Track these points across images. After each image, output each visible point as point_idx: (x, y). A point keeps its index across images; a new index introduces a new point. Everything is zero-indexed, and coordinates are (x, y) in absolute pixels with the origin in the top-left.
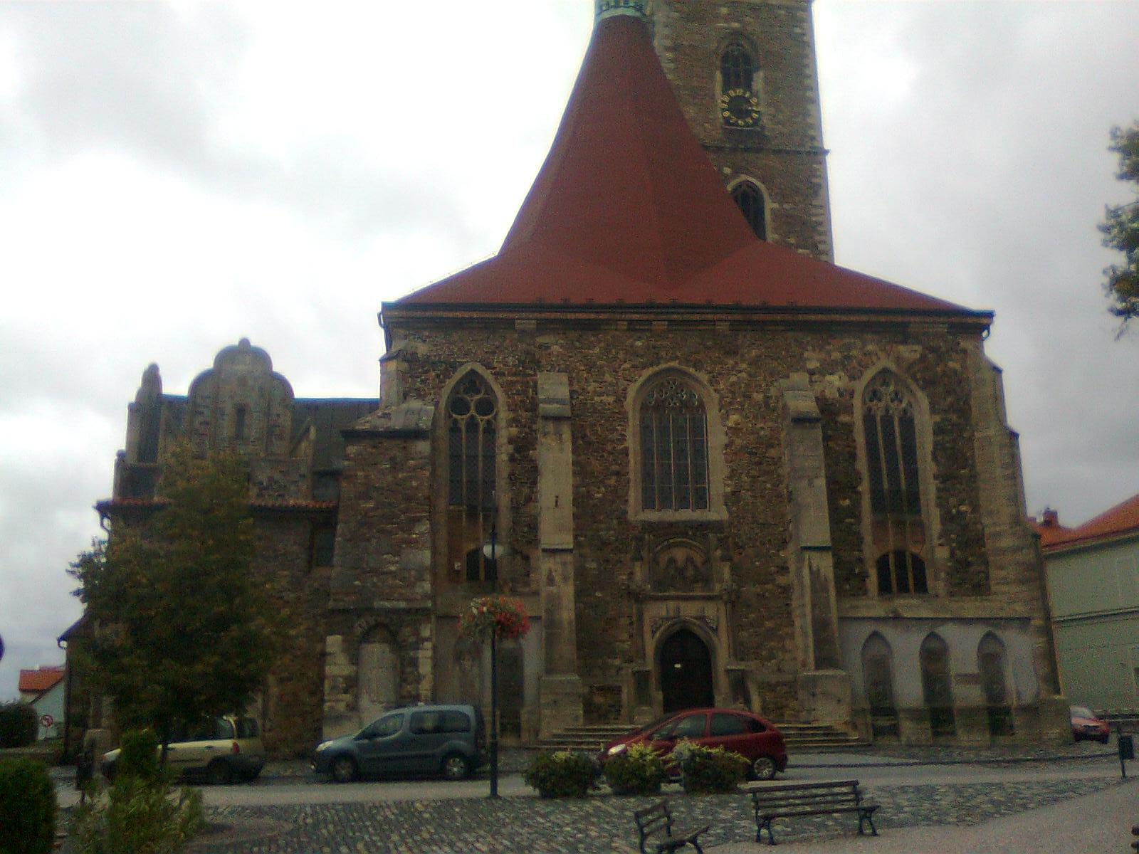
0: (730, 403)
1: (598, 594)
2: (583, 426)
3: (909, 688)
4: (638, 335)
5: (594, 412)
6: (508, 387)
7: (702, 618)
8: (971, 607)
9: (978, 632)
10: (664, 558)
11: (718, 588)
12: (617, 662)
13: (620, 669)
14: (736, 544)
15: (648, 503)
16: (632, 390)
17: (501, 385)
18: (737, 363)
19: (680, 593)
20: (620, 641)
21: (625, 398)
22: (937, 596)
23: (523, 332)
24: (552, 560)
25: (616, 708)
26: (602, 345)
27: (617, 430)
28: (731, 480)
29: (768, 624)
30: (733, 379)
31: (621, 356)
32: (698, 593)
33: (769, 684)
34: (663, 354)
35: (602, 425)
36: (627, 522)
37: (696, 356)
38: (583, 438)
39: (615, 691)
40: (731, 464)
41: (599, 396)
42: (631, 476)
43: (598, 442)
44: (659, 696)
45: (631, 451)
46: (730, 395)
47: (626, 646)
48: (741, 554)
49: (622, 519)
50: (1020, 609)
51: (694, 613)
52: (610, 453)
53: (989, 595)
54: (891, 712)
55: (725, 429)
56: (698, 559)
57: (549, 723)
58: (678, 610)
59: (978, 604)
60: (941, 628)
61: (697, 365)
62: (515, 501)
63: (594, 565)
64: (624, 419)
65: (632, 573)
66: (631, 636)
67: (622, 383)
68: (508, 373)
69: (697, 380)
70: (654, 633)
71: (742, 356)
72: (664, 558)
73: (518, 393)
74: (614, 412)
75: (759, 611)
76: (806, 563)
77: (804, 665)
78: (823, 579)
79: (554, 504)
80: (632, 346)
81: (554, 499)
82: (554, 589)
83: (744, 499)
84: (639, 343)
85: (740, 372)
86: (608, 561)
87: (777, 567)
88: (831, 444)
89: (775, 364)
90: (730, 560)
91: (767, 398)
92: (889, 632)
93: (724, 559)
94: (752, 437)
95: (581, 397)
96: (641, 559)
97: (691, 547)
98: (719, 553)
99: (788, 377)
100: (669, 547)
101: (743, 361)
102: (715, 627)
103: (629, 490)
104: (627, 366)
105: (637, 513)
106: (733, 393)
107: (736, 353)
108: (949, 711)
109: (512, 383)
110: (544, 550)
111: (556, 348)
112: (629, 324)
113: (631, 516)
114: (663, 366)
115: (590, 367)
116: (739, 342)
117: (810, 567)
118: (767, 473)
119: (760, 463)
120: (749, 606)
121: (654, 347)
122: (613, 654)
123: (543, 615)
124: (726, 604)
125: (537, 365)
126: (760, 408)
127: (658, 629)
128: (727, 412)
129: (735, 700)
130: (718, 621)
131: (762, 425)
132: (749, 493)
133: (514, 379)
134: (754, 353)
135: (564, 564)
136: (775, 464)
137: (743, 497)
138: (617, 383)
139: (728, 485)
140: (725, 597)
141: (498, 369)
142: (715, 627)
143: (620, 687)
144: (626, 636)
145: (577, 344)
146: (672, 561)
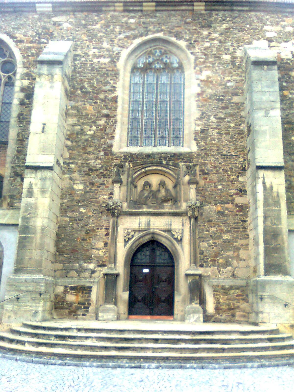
0: (204, 63)
1: (82, 210)
2: (81, 80)
4: (132, 14)
5: (92, 70)
6: (25, 51)
7: (169, 231)
10: (140, 183)
11: (184, 206)
12: (92, 266)
13: (93, 272)
14: (202, 171)
15: (133, 140)
16: (125, 53)
17: (20, 50)
18: (210, 33)
19: (151, 210)
20: (97, 249)
21: (118, 59)
23: (42, 14)
24: (33, 175)
25: (85, 306)
26: (103, 22)
27: (110, 83)
28: (202, 121)
29: (226, 237)
30: (207, 45)
31: (118, 29)
32: (167, 210)
33: (223, 288)
34: (151, 28)
35: (97, 80)
36: (112, 154)
37: (179, 29)
38: (81, 89)
39: (87, 290)
40: (202, 109)
41: (98, 58)
42: (119, 118)
43: (93, 92)
44: (126, 296)
45: (119, 100)
46: (204, 57)
47: (101, 253)
48: (206, 179)
49: (108, 151)
51: (163, 227)
52: (102, 100)
55: (198, 82)
56: (170, 184)
57: (9, 317)
58: (149, 224)
61: (178, 36)
62: (20, 135)
63: (81, 187)
64: (116, 74)
65: (112, 194)
66: (106, 244)
67: (116, 49)
68: (27, 41)
69: (178, 47)
70: (126, 242)
71: (215, 28)
72: (140, 183)
73: (33, 55)
74: (107, 70)
75: (219, 226)
76: (260, 181)
77: (255, 271)
78: (275, 194)
79: (41, 130)
80: (127, 23)
81: (42, 126)
82: (31, 200)
83: (211, 136)
84: (132, 21)
85: (213, 39)
86: (92, 184)
87: (237, 190)
88: (286, 93)
89: (241, 34)
90: (197, 183)
91: (233, 59)
93: (190, 183)
94: (220, 88)
95: (83, 59)
96: (120, 182)
97: (164, 174)
98: (187, 178)
99: (250, 43)
100: (146, 174)
101: (215, 31)
102: (179, 238)
103: (115, 128)
104: (122, 36)
105: (120, 145)
106: (206, 55)
107: (210, 27)
109: (30, 48)
110: (28, 167)
111: (66, 25)
112: (124, 6)
113: (115, 149)
114: (150, 36)
115: (92, 36)
116: (213, 19)
117: (264, 183)
118: (231, 115)
119: (227, 108)
120: (210, 221)
121: (144, 23)
122: (89, 259)
123: (20, 222)
124: (190, 218)
125: (51, 36)
126: (227, 66)
127: (129, 239)
128: (201, 68)
129: (192, 300)
130: (182, 233)
131: (229, 78)
132: (216, 130)
133: (30, 45)
134: (224, 26)
135: (43, 179)
136: (239, 108)
137: (211, 134)
138: (112, 49)
139: (199, 125)
140: (190, 213)
141: (19, 39)
142: (179, 238)
143: (91, 287)
144: (101, 245)
145: (83, 22)
146: (147, 184)
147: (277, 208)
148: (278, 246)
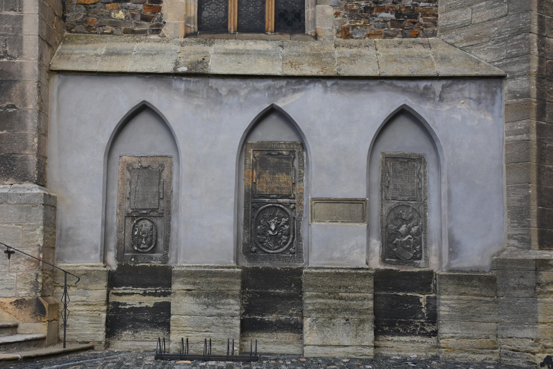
3: (206, 228)
8: (378, 55)
9: (378, 105)
22: (316, 37)
50: (485, 61)
53: (434, 34)
54: (162, 278)
59: (394, 51)
60: (298, 96)
92: (171, 103)
108: (293, 279)
147: (12, 13)
148: (10, 110)
